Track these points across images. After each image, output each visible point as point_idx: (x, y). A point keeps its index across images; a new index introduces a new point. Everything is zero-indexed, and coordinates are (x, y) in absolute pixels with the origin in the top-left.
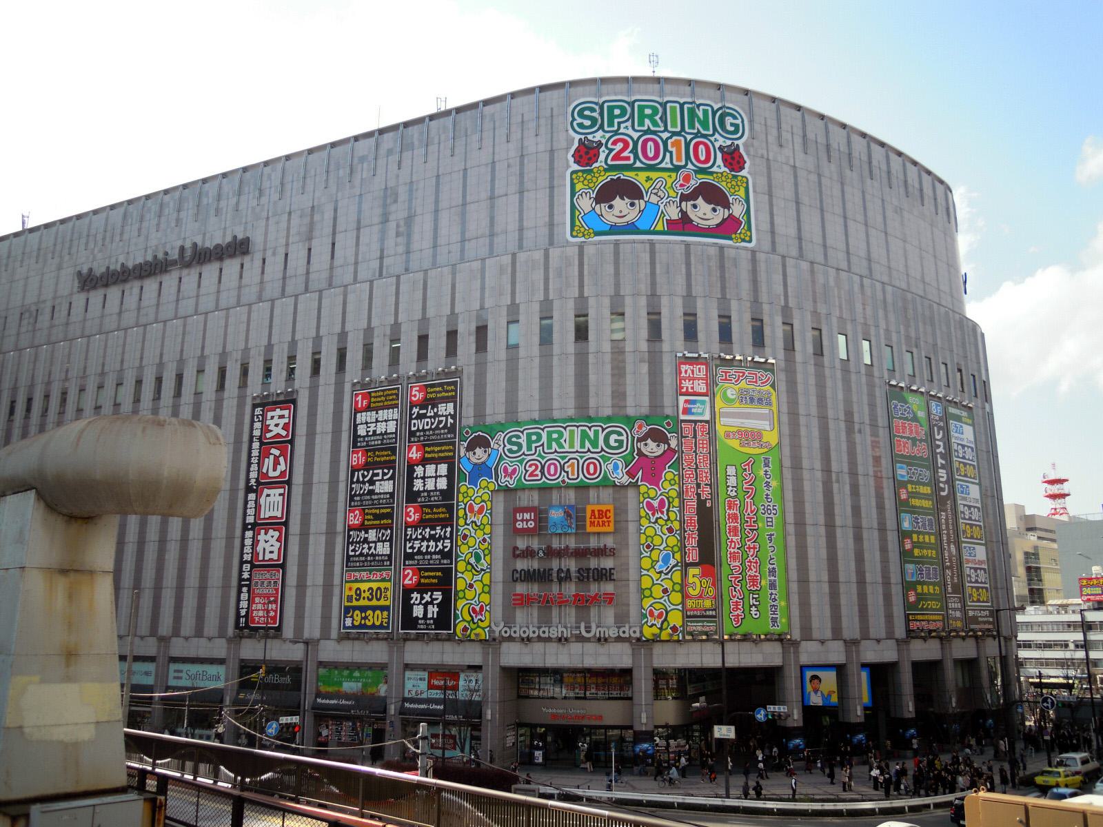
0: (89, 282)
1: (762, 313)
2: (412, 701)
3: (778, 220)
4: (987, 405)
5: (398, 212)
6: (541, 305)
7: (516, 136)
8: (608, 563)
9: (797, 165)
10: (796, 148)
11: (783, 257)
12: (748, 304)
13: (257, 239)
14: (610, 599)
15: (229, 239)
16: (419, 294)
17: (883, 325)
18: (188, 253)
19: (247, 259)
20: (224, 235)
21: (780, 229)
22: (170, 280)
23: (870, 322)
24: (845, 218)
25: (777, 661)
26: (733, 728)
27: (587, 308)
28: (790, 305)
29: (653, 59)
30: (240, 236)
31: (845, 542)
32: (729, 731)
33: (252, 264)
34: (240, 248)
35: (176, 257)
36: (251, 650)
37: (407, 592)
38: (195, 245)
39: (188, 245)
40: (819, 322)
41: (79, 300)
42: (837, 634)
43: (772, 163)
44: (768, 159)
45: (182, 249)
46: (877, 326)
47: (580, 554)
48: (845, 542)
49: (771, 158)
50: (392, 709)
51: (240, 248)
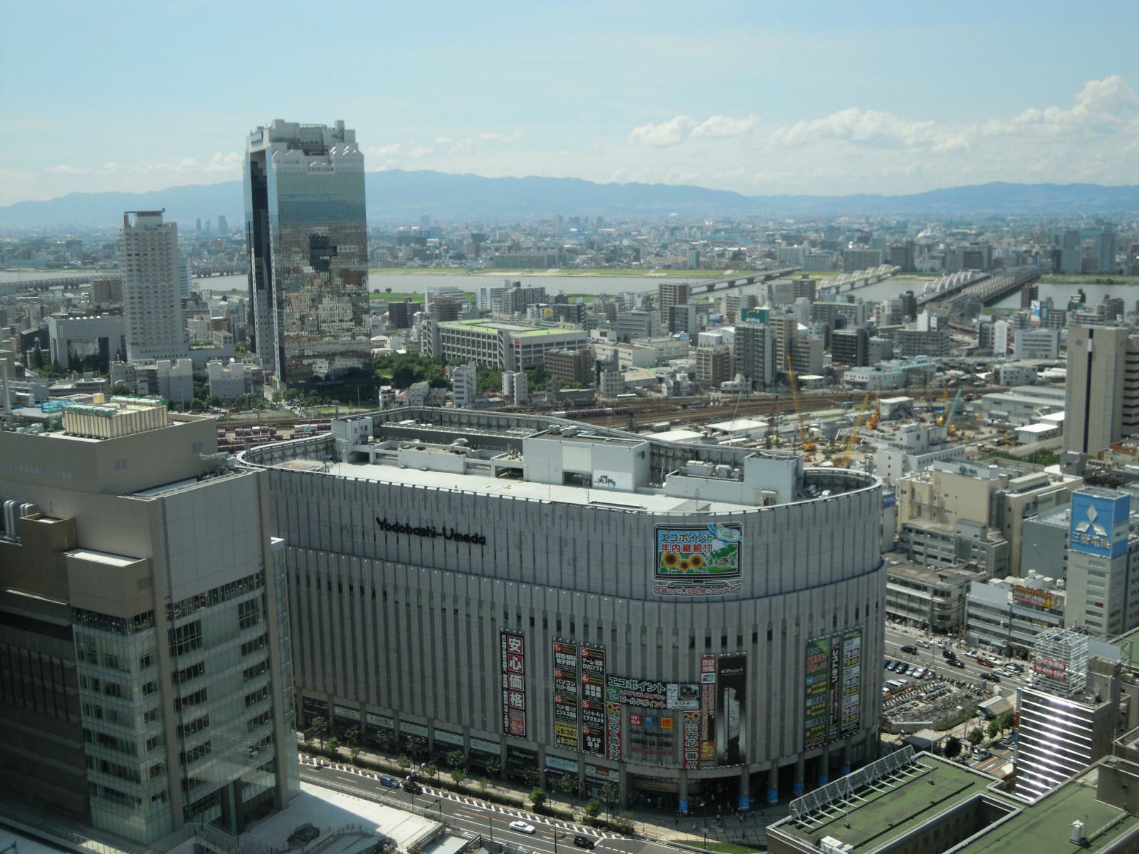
0: (384, 525)
2: (590, 777)
5: (568, 553)
7: (627, 533)
8: (670, 740)
13: (490, 539)
14: (670, 753)
16: (583, 605)
19: (485, 547)
22: (440, 542)
25: (740, 774)
31: (775, 721)
34: (480, 540)
36: (511, 741)
37: (585, 736)
38: (452, 530)
41: (381, 534)
42: (768, 758)
47: (658, 735)
48: (775, 721)
50: (581, 780)
51: (480, 540)
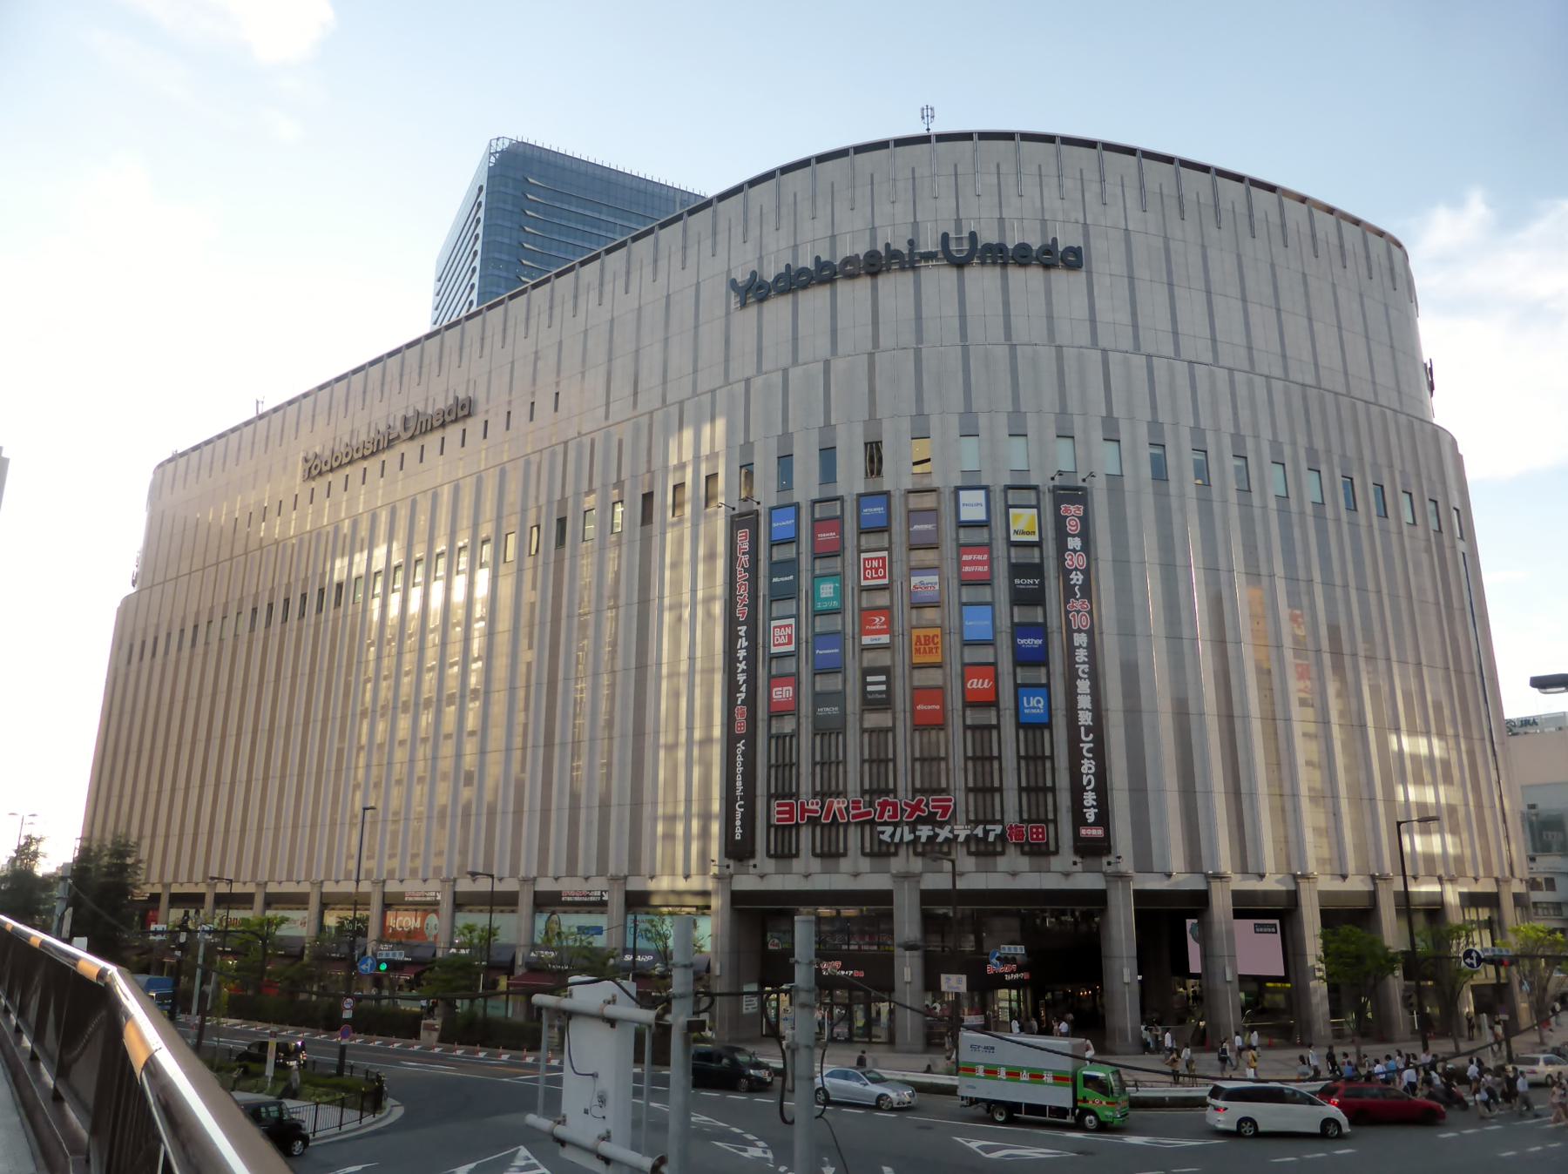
1: (1073, 429)
3: (1100, 304)
4: (1462, 546)
6: (778, 440)
7: (754, 232)
9: (1130, 228)
10: (1129, 205)
11: (1104, 351)
12: (1052, 417)
13: (480, 396)
15: (451, 401)
17: (1266, 434)
18: (412, 424)
20: (446, 399)
21: (1103, 315)
23: (1246, 430)
24: (1208, 292)
26: (964, 978)
27: (834, 439)
28: (1115, 415)
29: (927, 113)
30: (462, 396)
32: (959, 982)
33: (474, 425)
35: (399, 425)
39: (411, 413)
40: (1161, 434)
43: (1092, 230)
44: (1085, 224)
45: (406, 420)
46: (1257, 437)
49: (1088, 222)
